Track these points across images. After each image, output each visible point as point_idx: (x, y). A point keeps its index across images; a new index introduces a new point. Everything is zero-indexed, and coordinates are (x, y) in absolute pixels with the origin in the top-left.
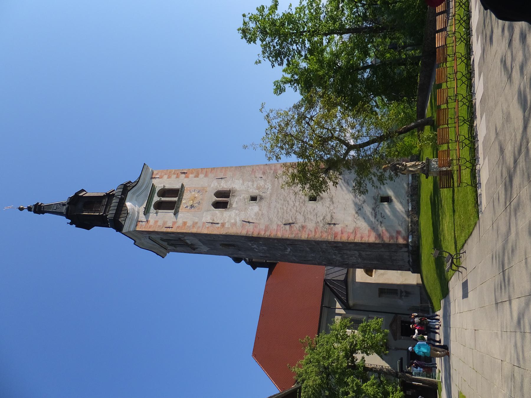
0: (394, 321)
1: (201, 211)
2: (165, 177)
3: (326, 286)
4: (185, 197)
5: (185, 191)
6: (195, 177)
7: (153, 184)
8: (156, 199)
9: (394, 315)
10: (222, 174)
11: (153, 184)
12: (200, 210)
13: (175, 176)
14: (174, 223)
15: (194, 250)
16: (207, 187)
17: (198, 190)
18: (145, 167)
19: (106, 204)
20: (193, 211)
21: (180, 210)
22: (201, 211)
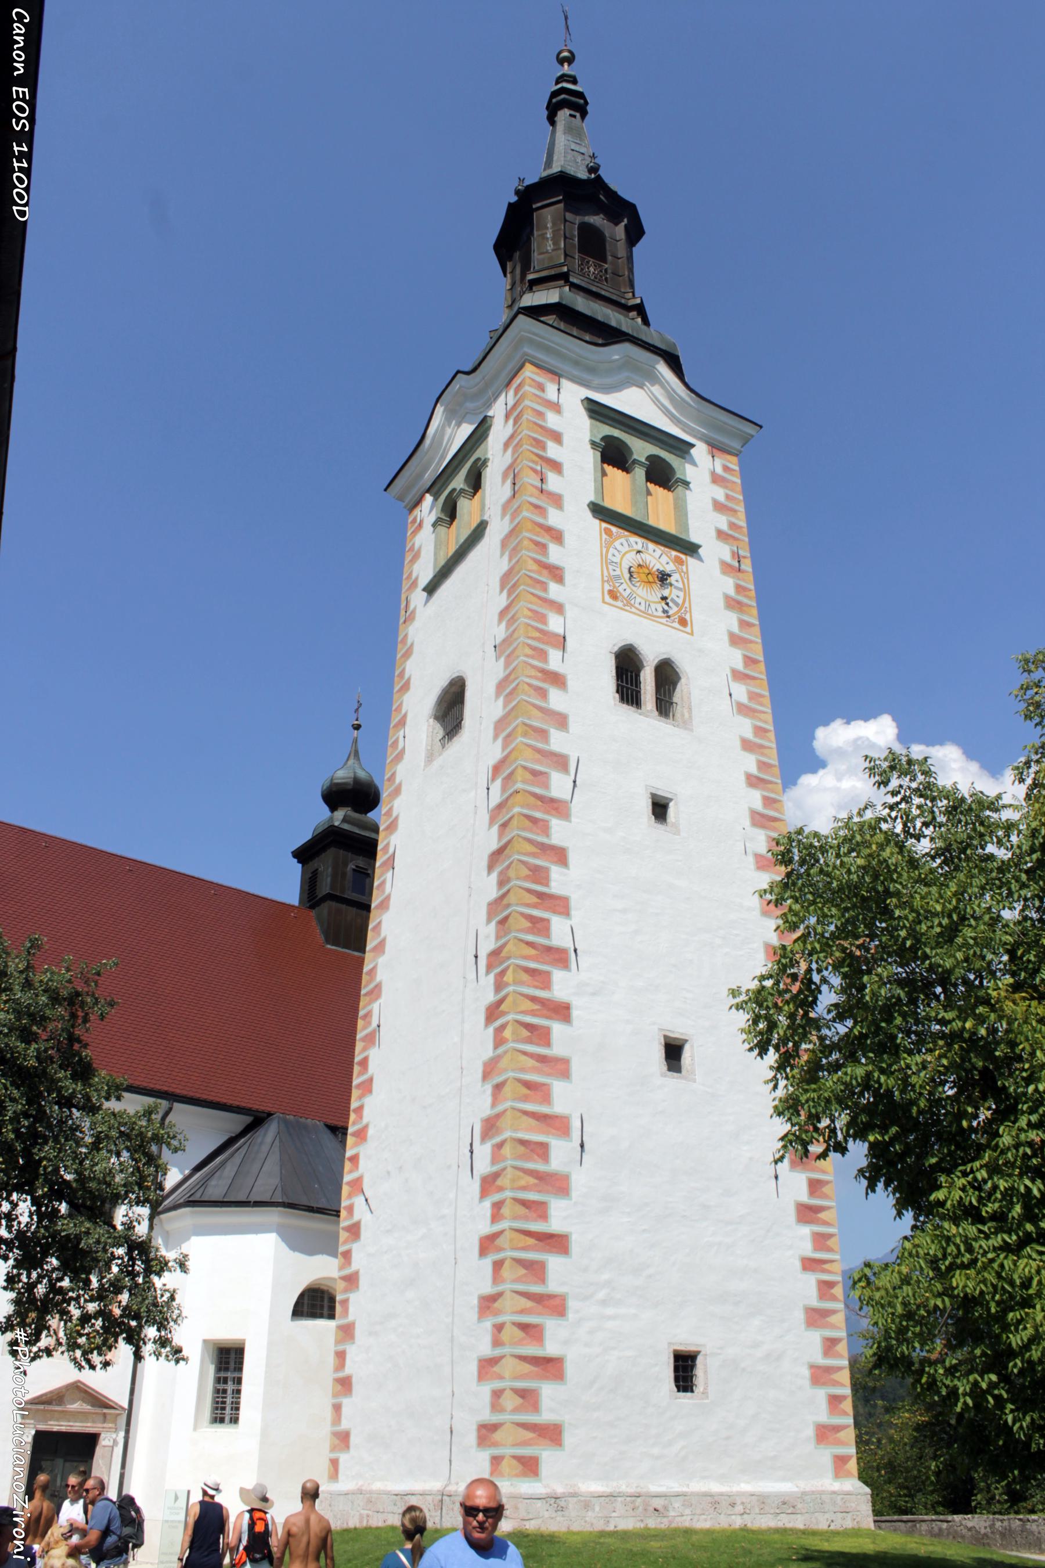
0: (100, 1402)
1: (604, 602)
2: (720, 494)
3: (248, 1119)
4: (651, 551)
5: (674, 553)
6: (727, 598)
7: (692, 446)
8: (641, 449)
9: (126, 1405)
10: (744, 699)
11: (692, 446)
12: (607, 598)
13: (725, 527)
14: (557, 500)
15: (424, 590)
16: (692, 634)
17: (680, 601)
18: (750, 429)
19: (603, 293)
20: (606, 573)
21: (604, 525)
22: (604, 602)
